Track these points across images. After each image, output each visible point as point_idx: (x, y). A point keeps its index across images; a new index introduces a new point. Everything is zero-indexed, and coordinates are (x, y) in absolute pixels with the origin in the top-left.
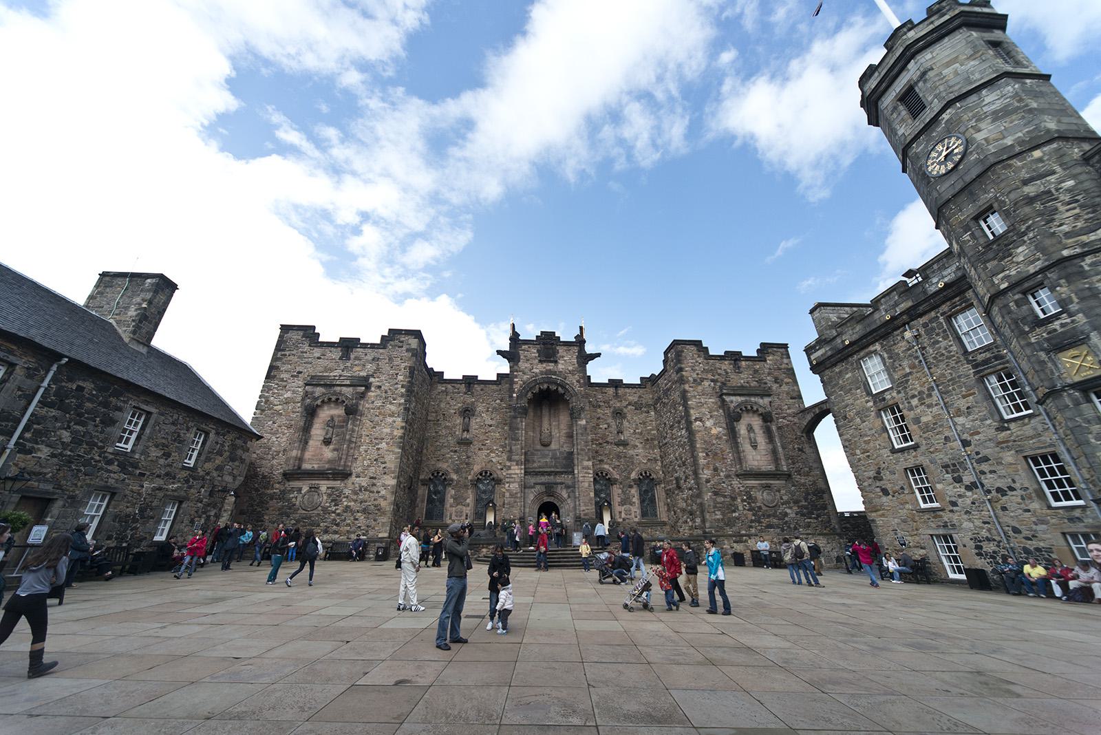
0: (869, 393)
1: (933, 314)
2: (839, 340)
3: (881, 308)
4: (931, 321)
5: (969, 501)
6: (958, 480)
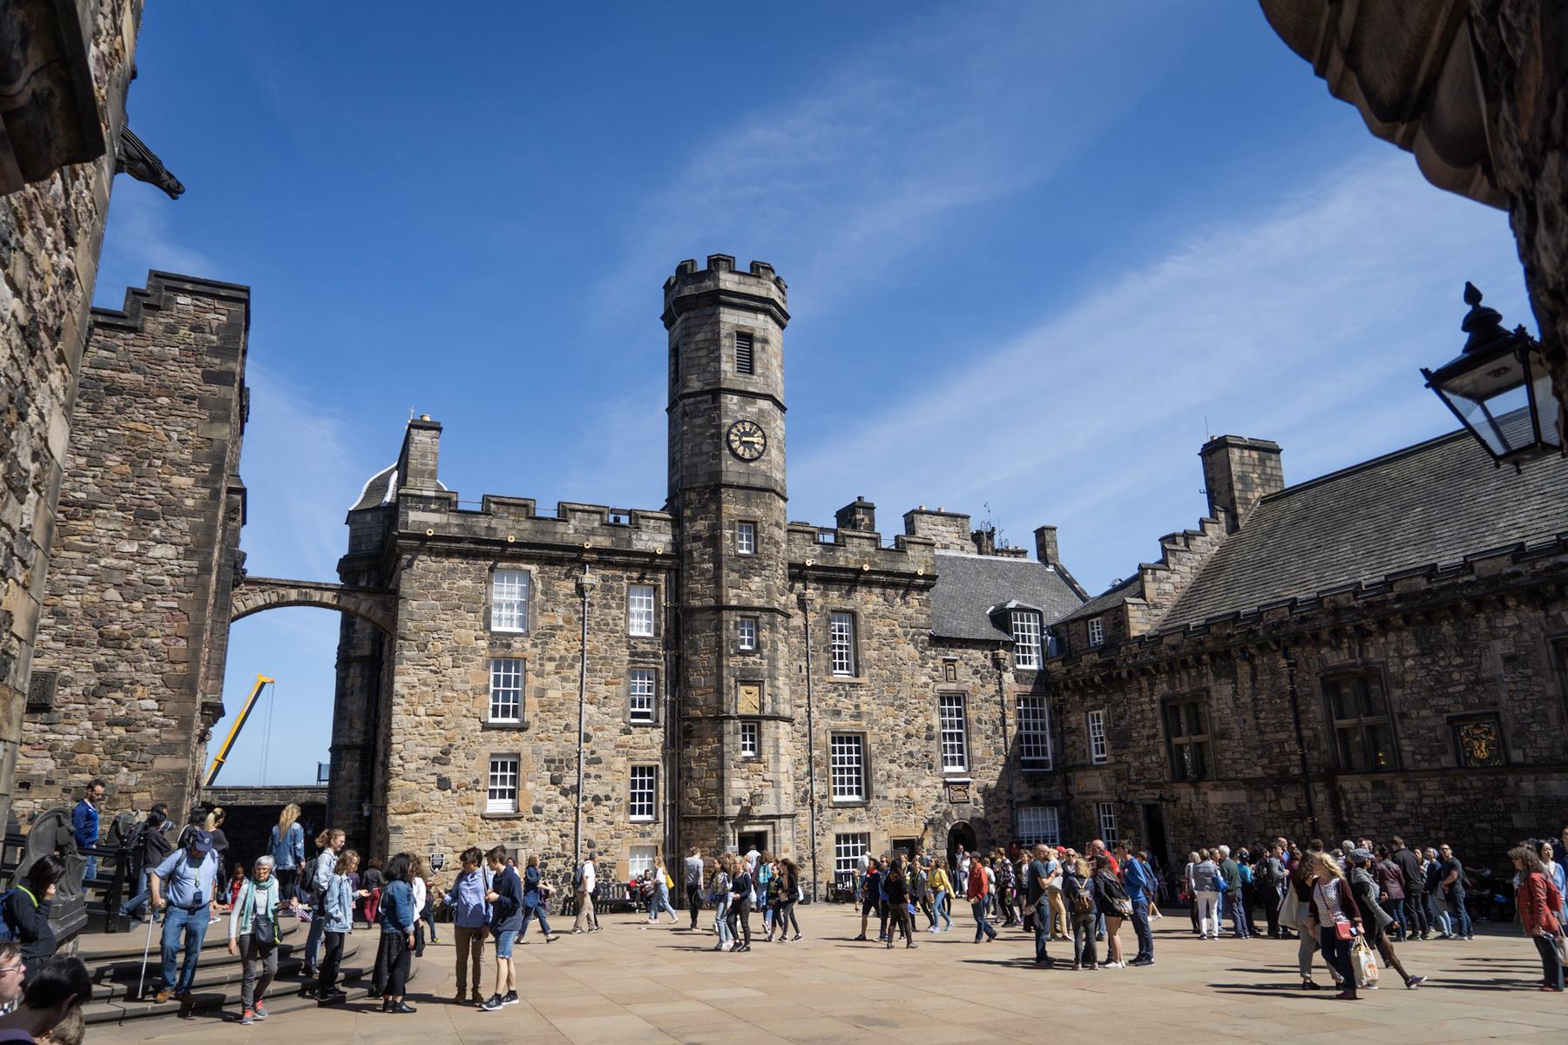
0: (487, 627)
1: (619, 573)
2: (483, 522)
3: (573, 521)
4: (613, 578)
5: (556, 808)
6: (554, 781)
